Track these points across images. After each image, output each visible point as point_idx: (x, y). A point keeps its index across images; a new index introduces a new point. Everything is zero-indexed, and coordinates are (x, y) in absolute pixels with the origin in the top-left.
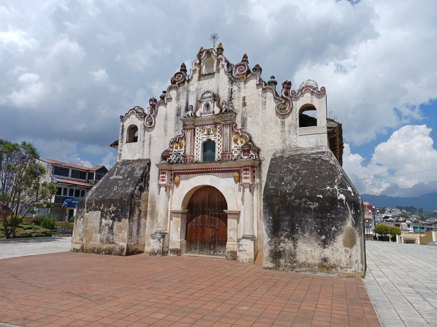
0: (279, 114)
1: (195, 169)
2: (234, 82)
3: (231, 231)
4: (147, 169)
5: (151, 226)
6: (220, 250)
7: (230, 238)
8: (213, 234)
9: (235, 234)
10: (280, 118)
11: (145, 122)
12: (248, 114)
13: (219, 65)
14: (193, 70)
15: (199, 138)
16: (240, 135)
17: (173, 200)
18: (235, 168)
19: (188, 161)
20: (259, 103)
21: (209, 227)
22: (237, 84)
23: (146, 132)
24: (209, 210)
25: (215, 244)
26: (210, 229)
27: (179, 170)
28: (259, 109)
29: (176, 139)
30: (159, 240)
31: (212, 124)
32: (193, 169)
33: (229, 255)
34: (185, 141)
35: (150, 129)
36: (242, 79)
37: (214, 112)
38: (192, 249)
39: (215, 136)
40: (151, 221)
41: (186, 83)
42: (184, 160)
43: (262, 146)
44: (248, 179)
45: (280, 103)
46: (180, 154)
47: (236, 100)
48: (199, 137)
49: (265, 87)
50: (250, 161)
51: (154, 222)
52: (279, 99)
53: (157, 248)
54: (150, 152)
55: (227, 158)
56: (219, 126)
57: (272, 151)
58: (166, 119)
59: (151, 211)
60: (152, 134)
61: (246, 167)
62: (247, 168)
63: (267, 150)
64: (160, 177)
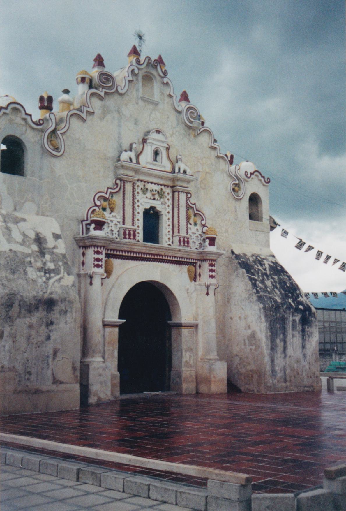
39: (162, 204)
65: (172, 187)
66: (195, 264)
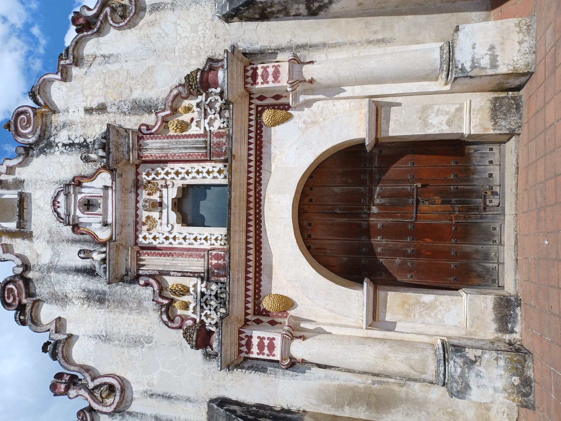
0: (133, 16)
1: (248, 243)
2: (51, 139)
3: (430, 121)
4: (236, 408)
5: (420, 411)
6: (487, 175)
7: (449, 123)
8: (438, 199)
9: (438, 110)
10: (142, 18)
11: (105, 409)
12: (124, 97)
13: (6, 181)
14: (4, 253)
15: (167, 234)
16: (168, 112)
17: (333, 321)
18: (250, 120)
19: (221, 262)
20: (104, 71)
21: (416, 213)
22: (55, 132)
23: (134, 408)
24: (366, 213)
25: (468, 194)
26: (424, 207)
27: (247, 296)
28: (117, 71)
29: (162, 305)
30: (473, 362)
31: (137, 195)
32: (247, 249)
33: (503, 123)
34: (168, 273)
35: (127, 393)
36: (47, 121)
37: (106, 188)
38: (488, 270)
39: (166, 186)
40: (400, 409)
41: (30, 275)
42: (219, 275)
43: (203, 53)
44: (280, 69)
45: (109, 18)
46: (203, 294)
47: (89, 134)
48: (163, 234)
49: (71, 58)
50: (232, 61)
51: (407, 394)
52: (101, 22)
53: (502, 372)
54: (188, 400)
55: (221, 139)
56: (144, 173)
57: (215, 26)
58: (106, 338)
59: (369, 406)
60: (142, 388)
61: (247, 77)
62: (249, 73)
63: (212, 41)
64: (261, 356)
65: (137, 166)
66: (260, 109)
